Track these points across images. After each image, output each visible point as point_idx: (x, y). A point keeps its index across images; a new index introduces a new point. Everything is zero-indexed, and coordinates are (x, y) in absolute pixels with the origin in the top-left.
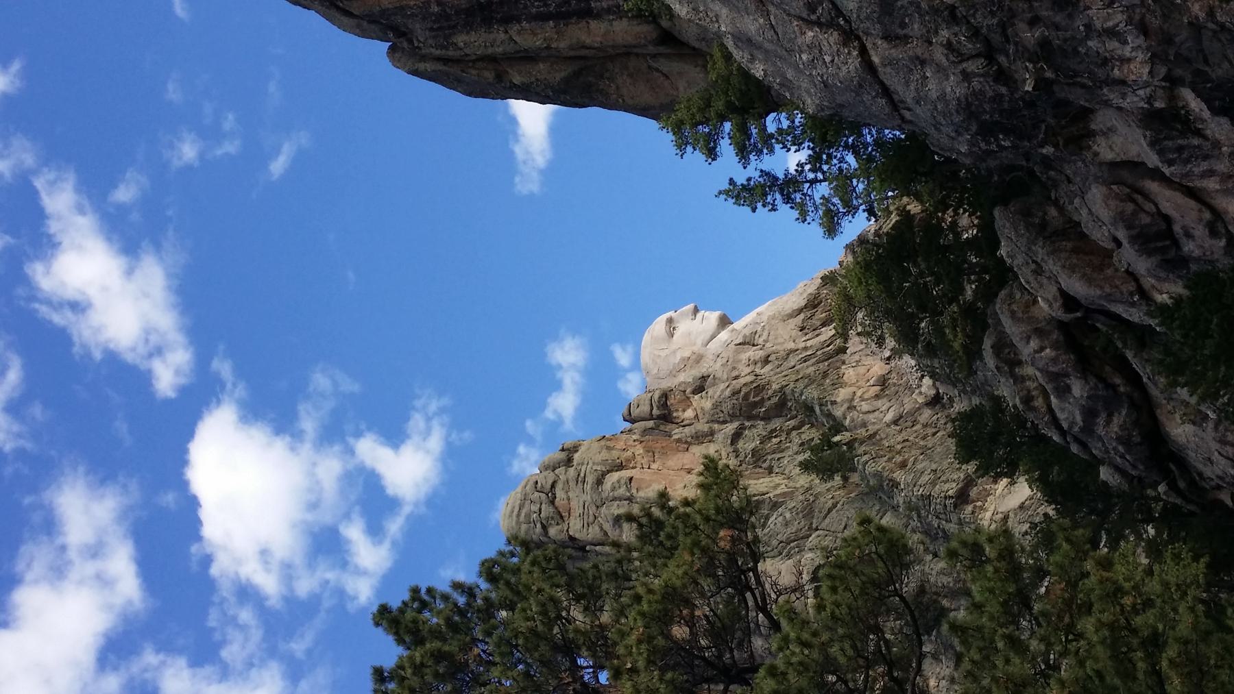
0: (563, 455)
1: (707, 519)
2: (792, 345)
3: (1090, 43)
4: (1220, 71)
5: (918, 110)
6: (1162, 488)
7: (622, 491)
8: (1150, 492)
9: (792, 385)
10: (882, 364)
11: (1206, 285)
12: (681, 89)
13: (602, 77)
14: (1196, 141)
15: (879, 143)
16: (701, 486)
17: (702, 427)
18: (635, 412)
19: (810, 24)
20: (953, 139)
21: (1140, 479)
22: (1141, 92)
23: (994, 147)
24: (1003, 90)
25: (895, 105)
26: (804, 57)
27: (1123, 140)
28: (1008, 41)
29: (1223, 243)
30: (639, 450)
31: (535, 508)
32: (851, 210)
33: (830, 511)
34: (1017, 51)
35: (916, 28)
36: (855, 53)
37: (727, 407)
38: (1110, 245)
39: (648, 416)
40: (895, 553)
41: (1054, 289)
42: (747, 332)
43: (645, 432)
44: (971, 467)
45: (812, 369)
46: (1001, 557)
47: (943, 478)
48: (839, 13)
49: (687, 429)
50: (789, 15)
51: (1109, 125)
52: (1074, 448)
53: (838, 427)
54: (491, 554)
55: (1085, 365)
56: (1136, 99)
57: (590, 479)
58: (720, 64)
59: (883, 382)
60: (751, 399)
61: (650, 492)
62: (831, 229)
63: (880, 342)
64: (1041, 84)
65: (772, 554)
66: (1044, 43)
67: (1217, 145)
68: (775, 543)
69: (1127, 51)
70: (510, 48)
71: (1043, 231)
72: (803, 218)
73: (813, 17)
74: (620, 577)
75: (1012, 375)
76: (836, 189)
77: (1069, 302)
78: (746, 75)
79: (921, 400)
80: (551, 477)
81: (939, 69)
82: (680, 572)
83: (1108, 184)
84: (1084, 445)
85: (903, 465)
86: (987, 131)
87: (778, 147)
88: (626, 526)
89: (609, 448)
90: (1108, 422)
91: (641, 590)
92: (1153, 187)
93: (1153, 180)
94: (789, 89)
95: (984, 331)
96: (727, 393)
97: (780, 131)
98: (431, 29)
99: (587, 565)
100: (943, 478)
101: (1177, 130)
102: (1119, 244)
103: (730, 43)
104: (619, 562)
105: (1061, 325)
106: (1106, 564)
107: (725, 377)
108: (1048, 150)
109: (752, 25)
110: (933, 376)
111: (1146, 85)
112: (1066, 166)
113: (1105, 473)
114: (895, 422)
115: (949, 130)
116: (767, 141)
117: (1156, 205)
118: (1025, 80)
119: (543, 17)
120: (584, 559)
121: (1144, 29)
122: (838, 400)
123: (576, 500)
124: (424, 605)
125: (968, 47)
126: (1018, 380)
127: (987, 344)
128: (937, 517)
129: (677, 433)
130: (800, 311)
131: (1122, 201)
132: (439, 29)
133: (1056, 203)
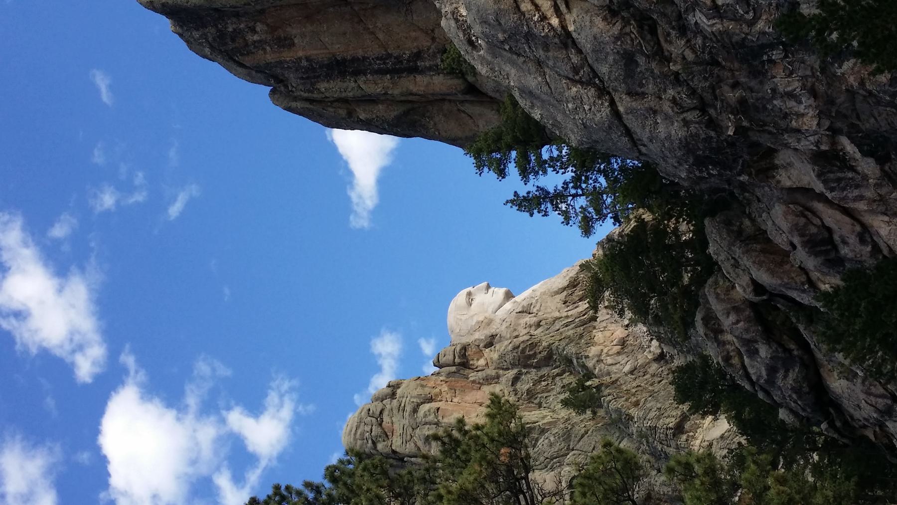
0: (389, 390)
1: (492, 440)
2: (557, 314)
3: (775, 102)
4: (868, 125)
5: (651, 146)
6: (824, 426)
7: (431, 418)
8: (814, 428)
9: (557, 343)
10: (623, 330)
11: (856, 278)
12: (481, 126)
13: (424, 116)
14: (850, 175)
15: (623, 169)
16: (488, 415)
17: (491, 372)
18: (443, 360)
19: (574, 82)
20: (676, 167)
21: (808, 419)
22: (811, 138)
23: (705, 174)
24: (713, 134)
25: (634, 142)
26: (570, 105)
27: (798, 172)
28: (716, 98)
29: (869, 248)
30: (445, 388)
31: (368, 428)
32: (602, 217)
33: (582, 436)
34: (723, 106)
35: (650, 88)
36: (607, 104)
37: (509, 358)
38: (788, 248)
39: (451, 363)
40: (630, 468)
41: (746, 278)
42: (525, 303)
43: (449, 375)
44: (685, 407)
45: (570, 333)
46: (706, 473)
47: (666, 414)
48: (595, 74)
50: (559, 75)
51: (788, 161)
52: (761, 395)
53: (589, 375)
54: (334, 461)
55: (769, 334)
56: (807, 143)
57: (408, 408)
58: (510, 109)
59: (623, 343)
60: (527, 353)
61: (450, 419)
62: (587, 229)
63: (621, 314)
64: (739, 130)
65: (540, 467)
66: (742, 101)
67: (865, 177)
68: (542, 459)
69: (801, 109)
70: (359, 93)
71: (740, 236)
72: (567, 220)
73: (577, 78)
74: (428, 481)
75: (716, 339)
76: (591, 201)
77: (758, 288)
78: (528, 117)
79: (650, 357)
80: (380, 406)
81: (667, 117)
82: (471, 478)
83: (786, 203)
84: (767, 393)
85: (636, 404)
86: (700, 163)
87: (550, 170)
88: (434, 444)
89: (422, 386)
90: (785, 377)
91: (442, 491)
92: (819, 206)
93: (819, 202)
94: (559, 129)
95: (696, 307)
96: (510, 348)
97: (551, 158)
98: (302, 78)
99: (404, 472)
100: (666, 414)
101: (837, 166)
102: (794, 247)
103: (517, 95)
104: (427, 470)
105: (752, 305)
106: (781, 481)
108: (744, 178)
109: (533, 82)
110: (659, 339)
111: (815, 133)
112: (756, 189)
113: (783, 414)
114: (632, 372)
115: (673, 161)
116: (542, 166)
117: (821, 220)
118: (728, 127)
119: (382, 72)
120: (402, 467)
121: (813, 93)
123: (398, 423)
124: (283, 498)
125: (688, 102)
126: (722, 344)
127: (698, 317)
129: (473, 376)
130: (564, 289)
131: (797, 216)
132: (308, 78)
133: (749, 216)
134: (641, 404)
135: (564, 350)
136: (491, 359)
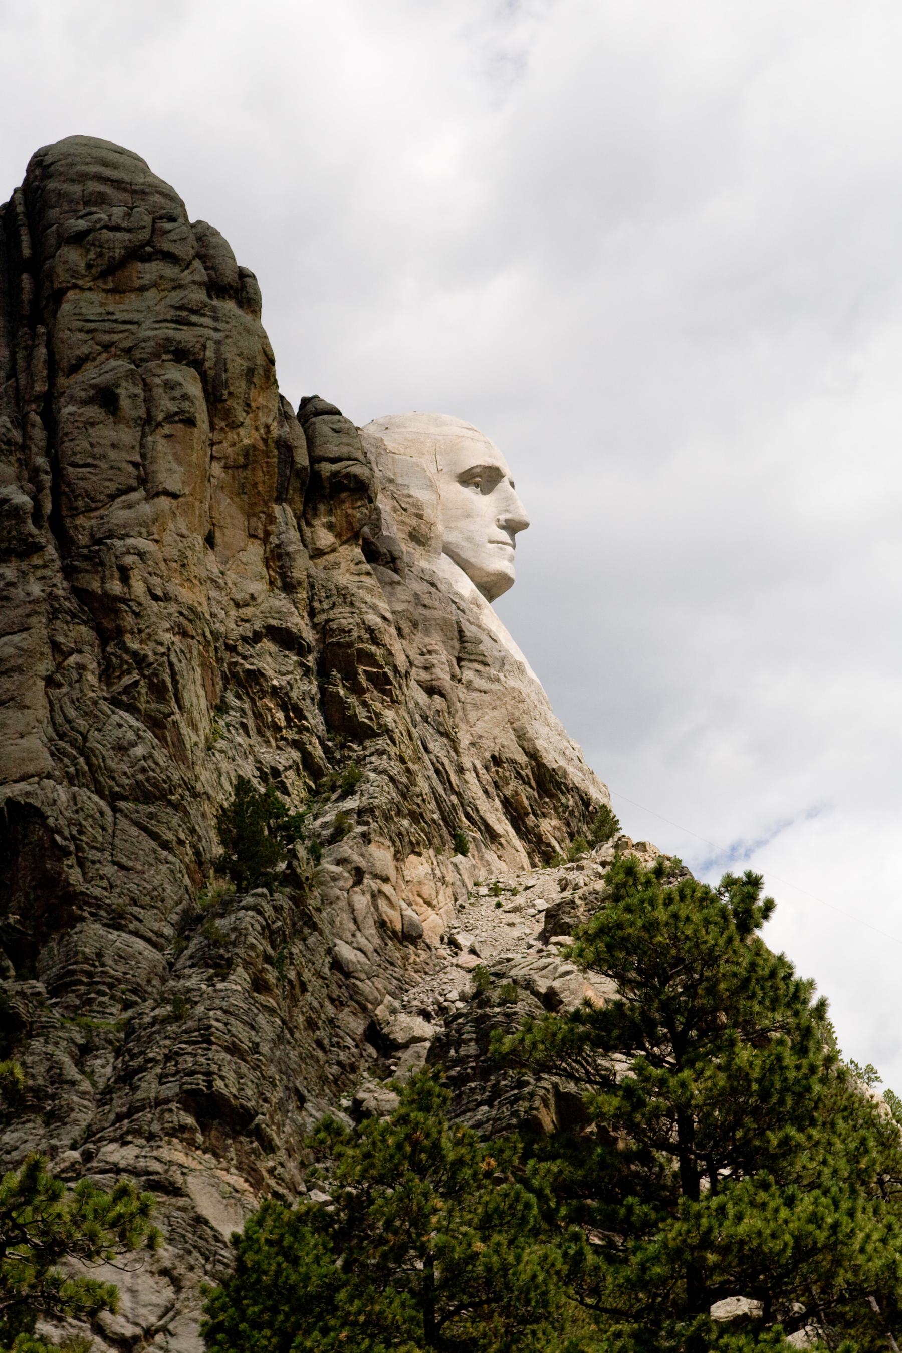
0: (230, 277)
2: (464, 740)
7: (166, 404)
9: (393, 750)
10: (441, 930)
17: (302, 566)
18: (322, 425)
30: (248, 437)
33: (154, 836)
37: (343, 618)
39: (319, 452)
42: (486, 646)
43: (285, 448)
45: (423, 786)
47: (244, 1068)
49: (294, 535)
60: (361, 669)
65: (60, 719)
68: (82, 723)
79: (381, 1011)
80: (184, 250)
85: (259, 985)
96: (373, 619)
107: (399, 607)
114: (337, 965)
122: (372, 848)
123: (145, 312)
128: (168, 1058)
130: (533, 755)
134: (261, 998)
135: (375, 770)
136: (336, 565)
